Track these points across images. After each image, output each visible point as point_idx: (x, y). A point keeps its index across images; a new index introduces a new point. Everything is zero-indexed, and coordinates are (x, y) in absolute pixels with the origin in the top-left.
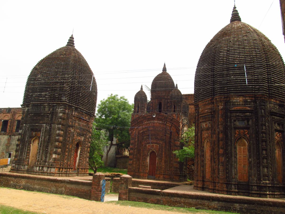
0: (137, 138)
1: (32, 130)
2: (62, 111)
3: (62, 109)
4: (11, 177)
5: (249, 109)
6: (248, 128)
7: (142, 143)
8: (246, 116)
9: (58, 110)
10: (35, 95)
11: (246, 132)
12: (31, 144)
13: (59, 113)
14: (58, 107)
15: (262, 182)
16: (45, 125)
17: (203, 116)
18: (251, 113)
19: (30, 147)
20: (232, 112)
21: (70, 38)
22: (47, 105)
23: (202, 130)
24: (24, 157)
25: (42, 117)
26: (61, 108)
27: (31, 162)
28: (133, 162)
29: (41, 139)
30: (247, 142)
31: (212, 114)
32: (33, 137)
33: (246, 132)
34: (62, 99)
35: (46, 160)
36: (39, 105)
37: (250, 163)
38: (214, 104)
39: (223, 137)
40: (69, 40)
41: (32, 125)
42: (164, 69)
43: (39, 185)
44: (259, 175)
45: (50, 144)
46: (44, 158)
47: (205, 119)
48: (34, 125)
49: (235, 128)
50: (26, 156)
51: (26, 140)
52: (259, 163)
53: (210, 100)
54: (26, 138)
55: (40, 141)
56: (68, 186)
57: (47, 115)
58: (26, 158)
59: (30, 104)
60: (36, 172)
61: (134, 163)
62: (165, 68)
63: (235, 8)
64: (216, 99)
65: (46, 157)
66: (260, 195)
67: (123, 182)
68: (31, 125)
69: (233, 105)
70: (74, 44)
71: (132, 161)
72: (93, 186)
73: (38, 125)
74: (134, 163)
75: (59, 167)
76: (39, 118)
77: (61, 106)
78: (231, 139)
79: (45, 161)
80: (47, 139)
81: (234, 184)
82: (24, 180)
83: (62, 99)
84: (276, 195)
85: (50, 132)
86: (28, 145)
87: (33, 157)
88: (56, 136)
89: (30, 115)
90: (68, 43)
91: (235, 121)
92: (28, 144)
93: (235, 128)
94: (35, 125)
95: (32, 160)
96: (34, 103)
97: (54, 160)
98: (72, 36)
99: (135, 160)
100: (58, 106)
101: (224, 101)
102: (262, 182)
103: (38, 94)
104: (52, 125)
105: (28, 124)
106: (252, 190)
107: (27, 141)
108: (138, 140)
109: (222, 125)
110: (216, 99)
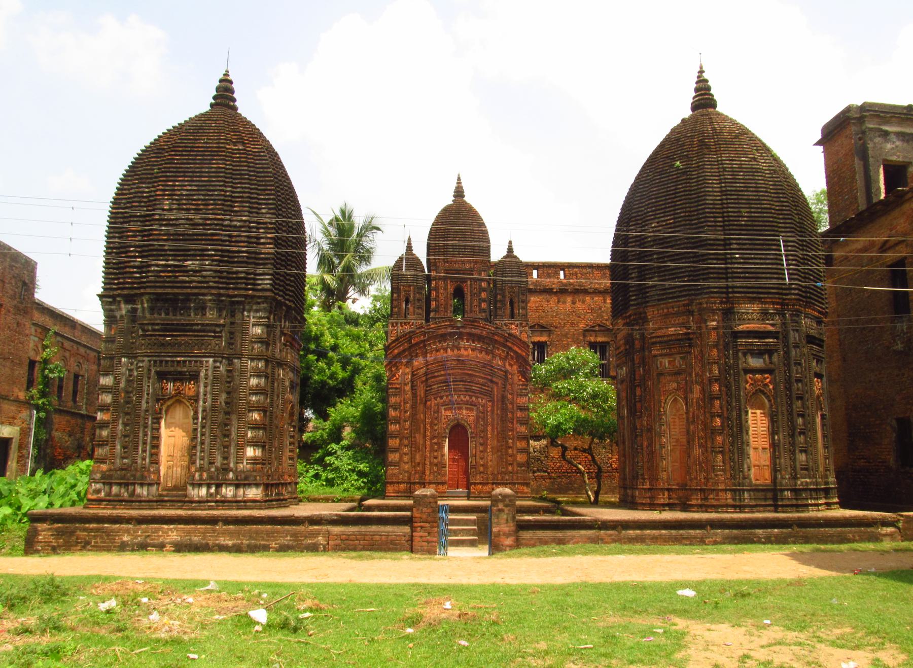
0: (408, 388)
1: (162, 376)
2: (260, 318)
3: (260, 314)
4: (121, 523)
5: (770, 328)
6: (770, 372)
7: (429, 403)
8: (767, 344)
9: (248, 316)
10: (157, 265)
11: (768, 380)
12: (161, 418)
13: (254, 325)
14: (247, 307)
15: (799, 482)
16: (211, 360)
17: (660, 342)
18: (777, 338)
19: (158, 429)
20: (736, 335)
21: (221, 81)
22: (210, 300)
23: (660, 374)
24: (144, 459)
25: (195, 336)
26: (257, 311)
27: (166, 475)
28: (401, 457)
29: (205, 402)
30: (770, 401)
31: (690, 339)
32: (169, 399)
33: (768, 380)
34: (260, 282)
35: (228, 464)
36: (179, 300)
37: (774, 446)
38: (692, 315)
39: (720, 390)
40: (218, 89)
41: (161, 362)
42: (459, 193)
43: (231, 535)
44: (794, 468)
45: (234, 417)
46: (219, 461)
47: (670, 349)
48: (167, 362)
49: (747, 371)
50: (152, 455)
51: (144, 405)
52: (793, 444)
53: (684, 305)
54: (144, 402)
55: (200, 409)
56: (336, 529)
57: (215, 332)
58: (151, 463)
59: (142, 294)
60: (199, 502)
61: (406, 458)
62: (462, 187)
63: (701, 72)
64: (701, 304)
65: (225, 458)
66: (798, 507)
67: (501, 506)
68: (155, 362)
69: (739, 319)
70: (234, 100)
71: (397, 454)
72: (416, 524)
73: (185, 362)
74: (406, 458)
75: (266, 481)
76: (186, 338)
77: (259, 303)
78: (739, 395)
79: (226, 470)
80: (223, 404)
81: (748, 490)
82: (172, 526)
83: (259, 285)
84: (821, 505)
85: (229, 382)
86: (153, 423)
87: (169, 459)
88: (250, 394)
89: (144, 330)
90: (215, 98)
91: (745, 354)
92: (153, 419)
93: (747, 371)
94: (173, 361)
95: (169, 467)
96: (160, 291)
97: (253, 463)
98: (226, 75)
99: (406, 450)
100: (249, 303)
101: (720, 310)
102: (799, 482)
103: (172, 263)
104: (236, 361)
105: (146, 359)
106: (782, 499)
107: (147, 411)
108: (414, 395)
109: (717, 363)
110: (701, 304)
